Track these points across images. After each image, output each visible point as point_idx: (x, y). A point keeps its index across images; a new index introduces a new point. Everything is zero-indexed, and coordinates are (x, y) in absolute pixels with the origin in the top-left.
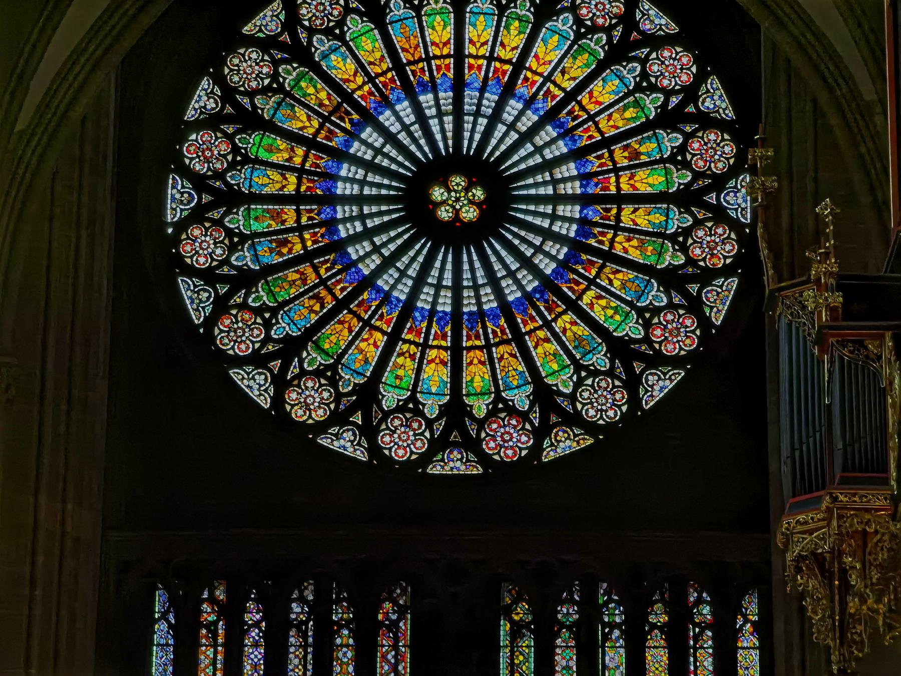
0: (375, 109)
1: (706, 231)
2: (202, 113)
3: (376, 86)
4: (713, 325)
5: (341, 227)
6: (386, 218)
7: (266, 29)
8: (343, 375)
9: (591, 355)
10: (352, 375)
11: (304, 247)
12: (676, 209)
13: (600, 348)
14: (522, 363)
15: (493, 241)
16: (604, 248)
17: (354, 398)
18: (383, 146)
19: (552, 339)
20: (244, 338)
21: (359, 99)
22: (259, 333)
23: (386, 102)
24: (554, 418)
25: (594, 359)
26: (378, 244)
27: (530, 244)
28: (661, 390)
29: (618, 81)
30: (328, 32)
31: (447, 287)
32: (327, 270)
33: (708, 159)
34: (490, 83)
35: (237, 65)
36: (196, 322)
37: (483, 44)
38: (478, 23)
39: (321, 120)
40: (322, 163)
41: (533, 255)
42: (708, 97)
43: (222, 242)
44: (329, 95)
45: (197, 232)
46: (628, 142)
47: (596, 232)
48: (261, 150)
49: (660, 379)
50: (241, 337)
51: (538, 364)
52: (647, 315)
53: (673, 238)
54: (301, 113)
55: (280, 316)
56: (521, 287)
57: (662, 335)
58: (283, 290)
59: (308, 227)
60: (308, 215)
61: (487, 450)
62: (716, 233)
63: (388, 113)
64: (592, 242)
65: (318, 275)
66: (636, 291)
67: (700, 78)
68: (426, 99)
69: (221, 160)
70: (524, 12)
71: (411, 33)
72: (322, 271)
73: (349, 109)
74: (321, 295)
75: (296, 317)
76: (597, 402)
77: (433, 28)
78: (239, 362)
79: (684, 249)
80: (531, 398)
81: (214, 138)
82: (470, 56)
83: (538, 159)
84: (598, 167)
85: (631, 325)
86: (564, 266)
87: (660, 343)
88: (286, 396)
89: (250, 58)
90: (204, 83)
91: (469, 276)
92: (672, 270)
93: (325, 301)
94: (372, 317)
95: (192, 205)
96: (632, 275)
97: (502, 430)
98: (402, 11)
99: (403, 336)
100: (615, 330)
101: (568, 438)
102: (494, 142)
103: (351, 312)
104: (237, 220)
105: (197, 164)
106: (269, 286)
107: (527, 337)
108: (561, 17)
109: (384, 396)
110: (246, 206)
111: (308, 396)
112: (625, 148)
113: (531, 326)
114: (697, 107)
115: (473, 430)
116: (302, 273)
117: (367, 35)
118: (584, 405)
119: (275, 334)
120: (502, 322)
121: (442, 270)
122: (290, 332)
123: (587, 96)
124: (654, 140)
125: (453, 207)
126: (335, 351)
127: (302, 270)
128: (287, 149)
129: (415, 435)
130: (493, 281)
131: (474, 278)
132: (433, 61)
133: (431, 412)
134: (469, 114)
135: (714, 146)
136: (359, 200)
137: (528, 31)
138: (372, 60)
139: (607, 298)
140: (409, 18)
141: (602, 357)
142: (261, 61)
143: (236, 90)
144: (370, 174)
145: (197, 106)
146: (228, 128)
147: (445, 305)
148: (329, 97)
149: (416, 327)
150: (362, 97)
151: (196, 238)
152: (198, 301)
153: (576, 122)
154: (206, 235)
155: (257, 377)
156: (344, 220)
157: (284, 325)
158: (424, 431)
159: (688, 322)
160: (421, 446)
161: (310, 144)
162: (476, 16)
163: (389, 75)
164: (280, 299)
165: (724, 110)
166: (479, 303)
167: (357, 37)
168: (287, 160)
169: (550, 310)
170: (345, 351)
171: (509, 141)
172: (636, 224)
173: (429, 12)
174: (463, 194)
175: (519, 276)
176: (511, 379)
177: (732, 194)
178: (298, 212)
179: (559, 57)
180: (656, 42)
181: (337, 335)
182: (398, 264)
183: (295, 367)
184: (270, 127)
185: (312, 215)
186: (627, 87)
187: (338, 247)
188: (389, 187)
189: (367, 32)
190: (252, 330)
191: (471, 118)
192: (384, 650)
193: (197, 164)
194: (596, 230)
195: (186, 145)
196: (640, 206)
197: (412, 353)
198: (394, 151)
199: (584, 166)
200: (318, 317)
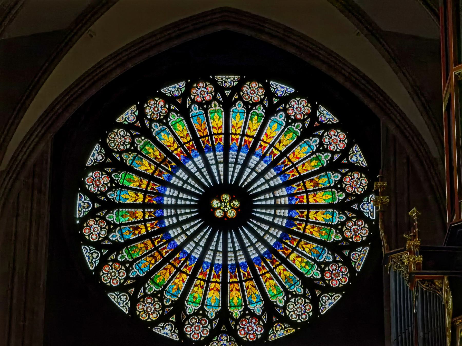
0: (184, 160)
1: (352, 223)
2: (95, 162)
3: (184, 148)
4: (356, 271)
5: (166, 220)
6: (189, 216)
7: (128, 120)
8: (166, 296)
9: (293, 286)
10: (171, 296)
11: (147, 230)
12: (337, 212)
13: (298, 283)
14: (258, 290)
15: (244, 228)
16: (300, 232)
17: (172, 308)
18: (188, 179)
19: (274, 278)
20: (115, 277)
21: (176, 155)
22: (123, 274)
23: (189, 157)
24: (275, 319)
25: (295, 289)
26: (185, 229)
27: (263, 230)
28: (330, 305)
29: (308, 147)
30: (160, 121)
31: (220, 251)
32: (159, 242)
33: (354, 187)
34: (242, 147)
35: (113, 138)
36: (91, 269)
37: (239, 128)
38: (236, 117)
39: (156, 166)
40: (156, 187)
41: (264, 235)
42: (354, 155)
43: (105, 228)
44: (160, 153)
45: (92, 223)
46: (313, 177)
47: (296, 223)
48: (125, 181)
49: (329, 298)
50: (114, 276)
51: (267, 291)
52: (323, 266)
53: (336, 227)
54: (146, 162)
55: (134, 266)
56: (258, 251)
57: (330, 277)
58: (136, 252)
59: (149, 220)
60: (149, 214)
61: (240, 335)
62: (358, 224)
63: (190, 162)
64: (294, 228)
65: (154, 245)
66: (316, 254)
67: (349, 146)
68: (210, 155)
69: (105, 186)
70: (260, 112)
71: (202, 122)
72: (156, 243)
73: (170, 160)
74: (155, 255)
75: (142, 267)
76: (297, 310)
77: (214, 119)
78: (112, 289)
79: (342, 232)
80: (263, 308)
81: (101, 175)
82: (233, 134)
83: (267, 186)
84: (298, 190)
85: (314, 271)
86: (280, 241)
87: (329, 281)
88: (137, 307)
89: (120, 135)
90: (97, 147)
91: (231, 246)
92: (335, 243)
93: (157, 258)
94: (181, 266)
95: (90, 209)
96: (315, 245)
97: (248, 325)
98: (197, 111)
99: (197, 277)
100: (306, 274)
101: (282, 329)
102: (244, 177)
103: (170, 263)
104: (112, 217)
105: (92, 188)
106: (129, 251)
107: (261, 277)
108: (279, 114)
109: (187, 307)
110: (117, 210)
111: (148, 307)
112: (311, 181)
113: (263, 271)
114: (348, 160)
115: (233, 325)
116: (146, 244)
117: (180, 123)
118: (290, 312)
119: (131, 275)
120: (248, 269)
121: (217, 242)
122: (139, 274)
123: (292, 154)
124: (326, 176)
125: (223, 210)
126: (162, 284)
127: (145, 242)
128: (138, 181)
129: (203, 327)
130: (244, 248)
131: (234, 247)
132: (213, 136)
133: (212, 315)
134: (232, 163)
135: (357, 180)
136: (176, 207)
137: (262, 121)
138: (182, 136)
139: (302, 257)
140: (201, 114)
141: (300, 288)
142: (125, 136)
143: (113, 151)
144: (181, 194)
145: (92, 159)
146: (108, 170)
147: (219, 260)
148: (160, 154)
149: (204, 271)
150: (177, 154)
151: (91, 226)
152: (92, 258)
153: (286, 168)
154: (96, 224)
155: (122, 297)
156: (167, 217)
157: (136, 270)
158: (208, 325)
159: (343, 270)
160: (206, 334)
161: (150, 178)
162: (236, 113)
164: (134, 257)
165: (362, 162)
166: (236, 260)
167: (175, 124)
168: (138, 186)
169: (272, 263)
170: (167, 284)
171: (252, 177)
172: (317, 220)
173: (211, 111)
174: (228, 204)
175: (257, 246)
176: (252, 299)
177: (366, 205)
178: (144, 213)
179: (277, 135)
180: (327, 127)
181: (163, 276)
182: (195, 240)
183: (141, 292)
184: (130, 169)
185: (151, 214)
186: (312, 150)
187: (164, 230)
188: (191, 200)
189: (180, 121)
190: (120, 273)
191: (233, 165)
193: (92, 188)
194: (296, 222)
195: (87, 178)
196: (319, 210)
197: (202, 285)
198: (193, 182)
199: (290, 190)
200: (153, 266)
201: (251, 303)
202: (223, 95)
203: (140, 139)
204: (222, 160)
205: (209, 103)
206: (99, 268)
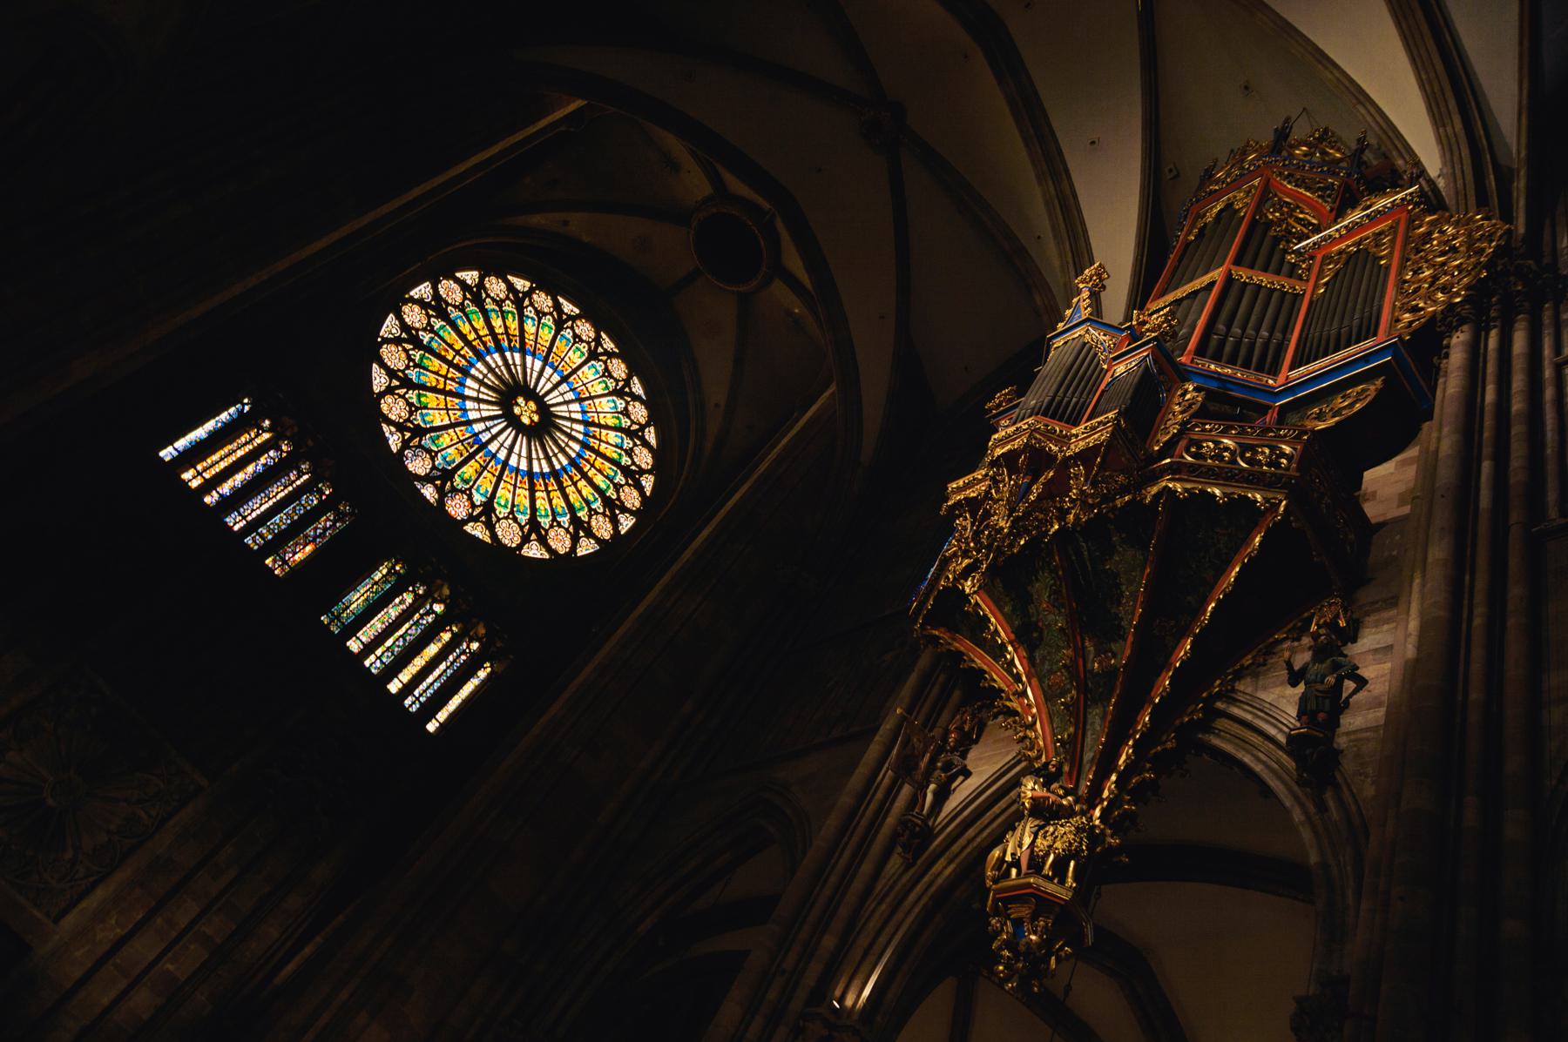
23: (534, 354)
30: (537, 312)
40: (489, 344)
45: (416, 310)
52: (555, 524)
55: (416, 370)
56: (519, 463)
68: (548, 371)
75: (422, 378)
78: (383, 365)
79: (590, 517)
83: (569, 431)
90: (475, 274)
96: (564, 505)
103: (445, 399)
104: (438, 324)
113: (508, 480)
120: (499, 467)
136: (491, 370)
143: (486, 290)
147: (485, 437)
148: (515, 329)
156: (477, 369)
159: (567, 542)
160: (421, 472)
163: (544, 348)
166: (497, 451)
169: (521, 482)
171: (563, 414)
180: (646, 444)
192: (319, 526)
194: (565, 476)
201: (477, 490)
202: (596, 348)
203: (511, 305)
204: (554, 382)
205: (582, 341)
206: (386, 341)
